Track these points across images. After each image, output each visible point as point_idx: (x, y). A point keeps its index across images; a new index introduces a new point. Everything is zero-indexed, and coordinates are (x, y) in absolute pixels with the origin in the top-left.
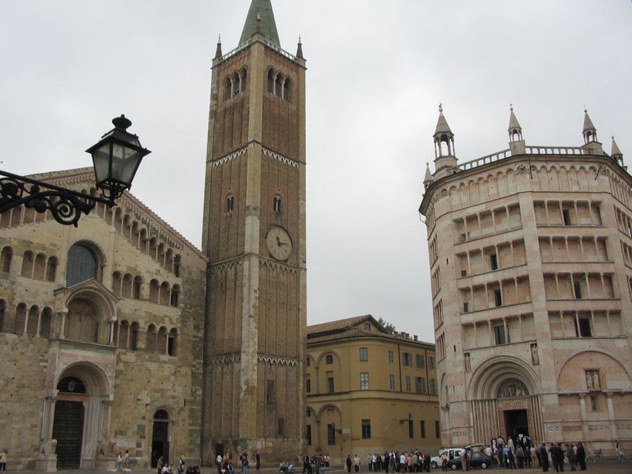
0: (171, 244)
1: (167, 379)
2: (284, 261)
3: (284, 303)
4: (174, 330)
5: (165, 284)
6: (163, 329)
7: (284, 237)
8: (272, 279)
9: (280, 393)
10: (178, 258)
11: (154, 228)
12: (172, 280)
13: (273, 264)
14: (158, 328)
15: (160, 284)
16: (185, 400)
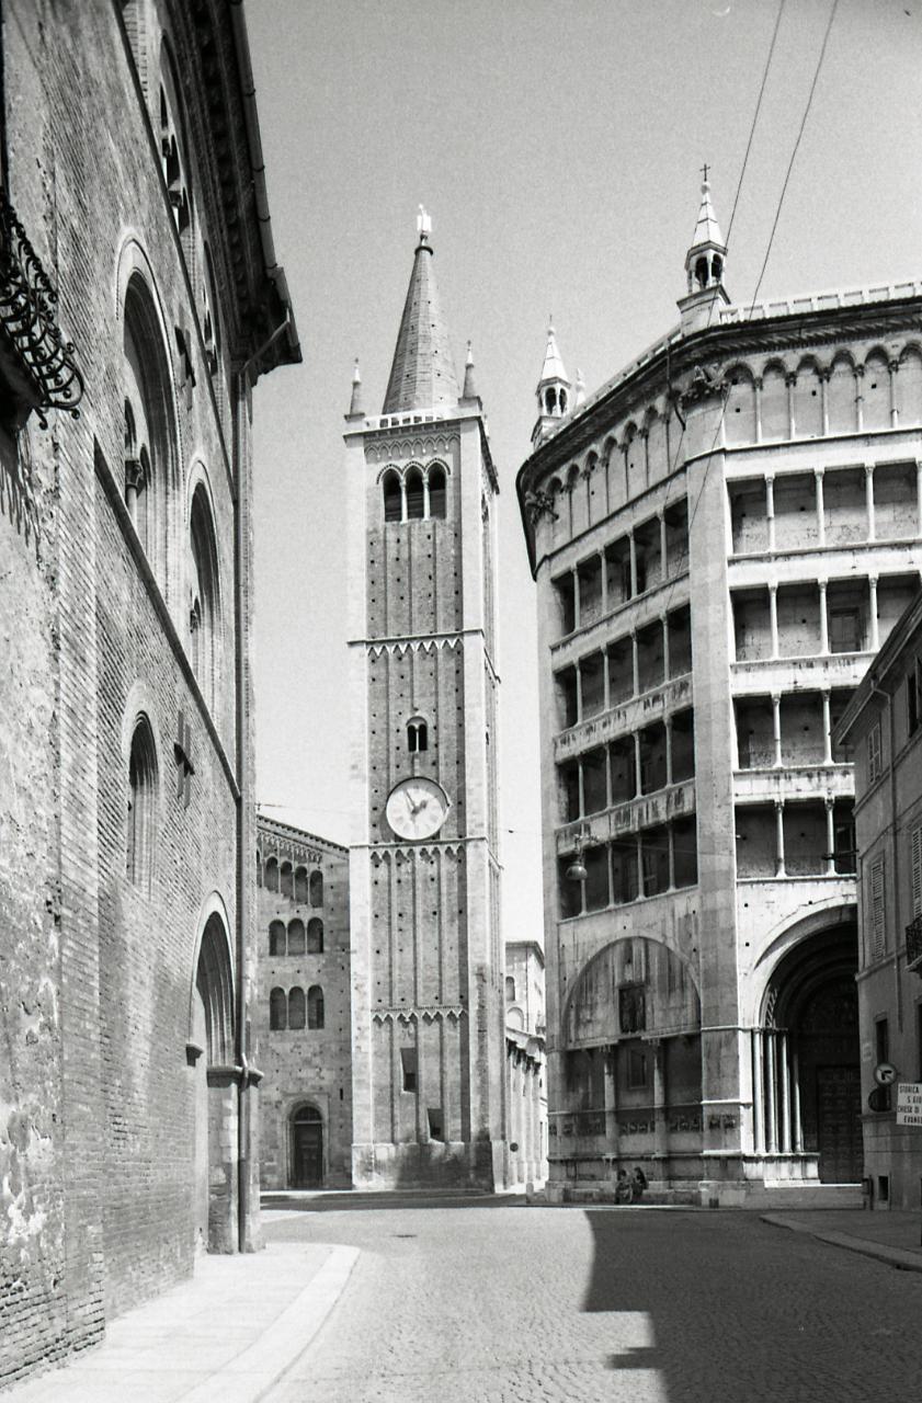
0: (298, 858)
1: (307, 1062)
2: (433, 837)
3: (435, 913)
4: (315, 990)
5: (296, 923)
6: (296, 991)
7: (419, 794)
8: (404, 878)
9: (427, 1070)
10: (318, 876)
11: (270, 843)
12: (306, 914)
13: (405, 850)
14: (287, 992)
15: (286, 925)
16: (341, 1091)
